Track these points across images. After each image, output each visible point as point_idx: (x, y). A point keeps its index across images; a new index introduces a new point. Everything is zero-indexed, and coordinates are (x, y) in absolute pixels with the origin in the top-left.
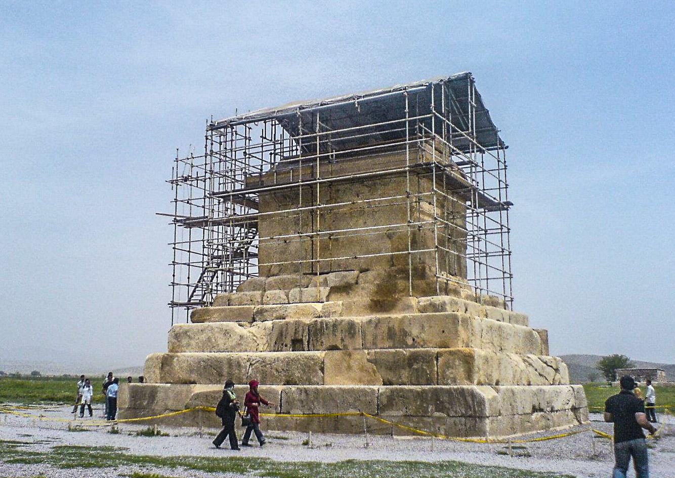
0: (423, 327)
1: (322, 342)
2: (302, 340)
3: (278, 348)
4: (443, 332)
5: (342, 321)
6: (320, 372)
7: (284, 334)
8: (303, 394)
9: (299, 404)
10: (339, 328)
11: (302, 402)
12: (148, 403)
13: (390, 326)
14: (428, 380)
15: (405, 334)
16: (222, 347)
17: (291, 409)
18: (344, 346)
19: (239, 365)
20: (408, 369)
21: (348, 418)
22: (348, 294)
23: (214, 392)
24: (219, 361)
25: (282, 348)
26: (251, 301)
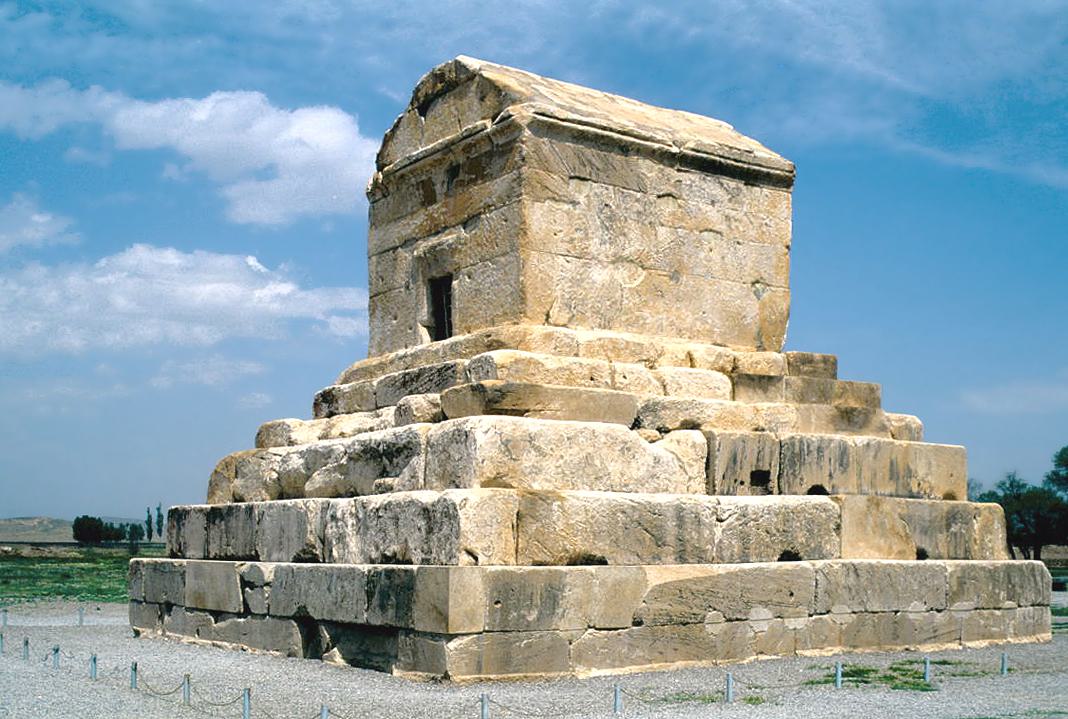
0: (930, 463)
1: (802, 479)
2: (768, 472)
3: (729, 489)
4: (952, 475)
5: (831, 441)
6: (834, 534)
7: (738, 459)
8: (851, 574)
9: (846, 596)
10: (826, 453)
11: (850, 589)
12: (540, 613)
13: (893, 457)
14: (967, 551)
15: (910, 473)
16: (616, 479)
17: (833, 604)
18: (833, 487)
19: (699, 521)
20: (945, 533)
21: (911, 616)
22: (765, 391)
23: (697, 581)
24: (655, 511)
25: (735, 489)
26: (592, 379)
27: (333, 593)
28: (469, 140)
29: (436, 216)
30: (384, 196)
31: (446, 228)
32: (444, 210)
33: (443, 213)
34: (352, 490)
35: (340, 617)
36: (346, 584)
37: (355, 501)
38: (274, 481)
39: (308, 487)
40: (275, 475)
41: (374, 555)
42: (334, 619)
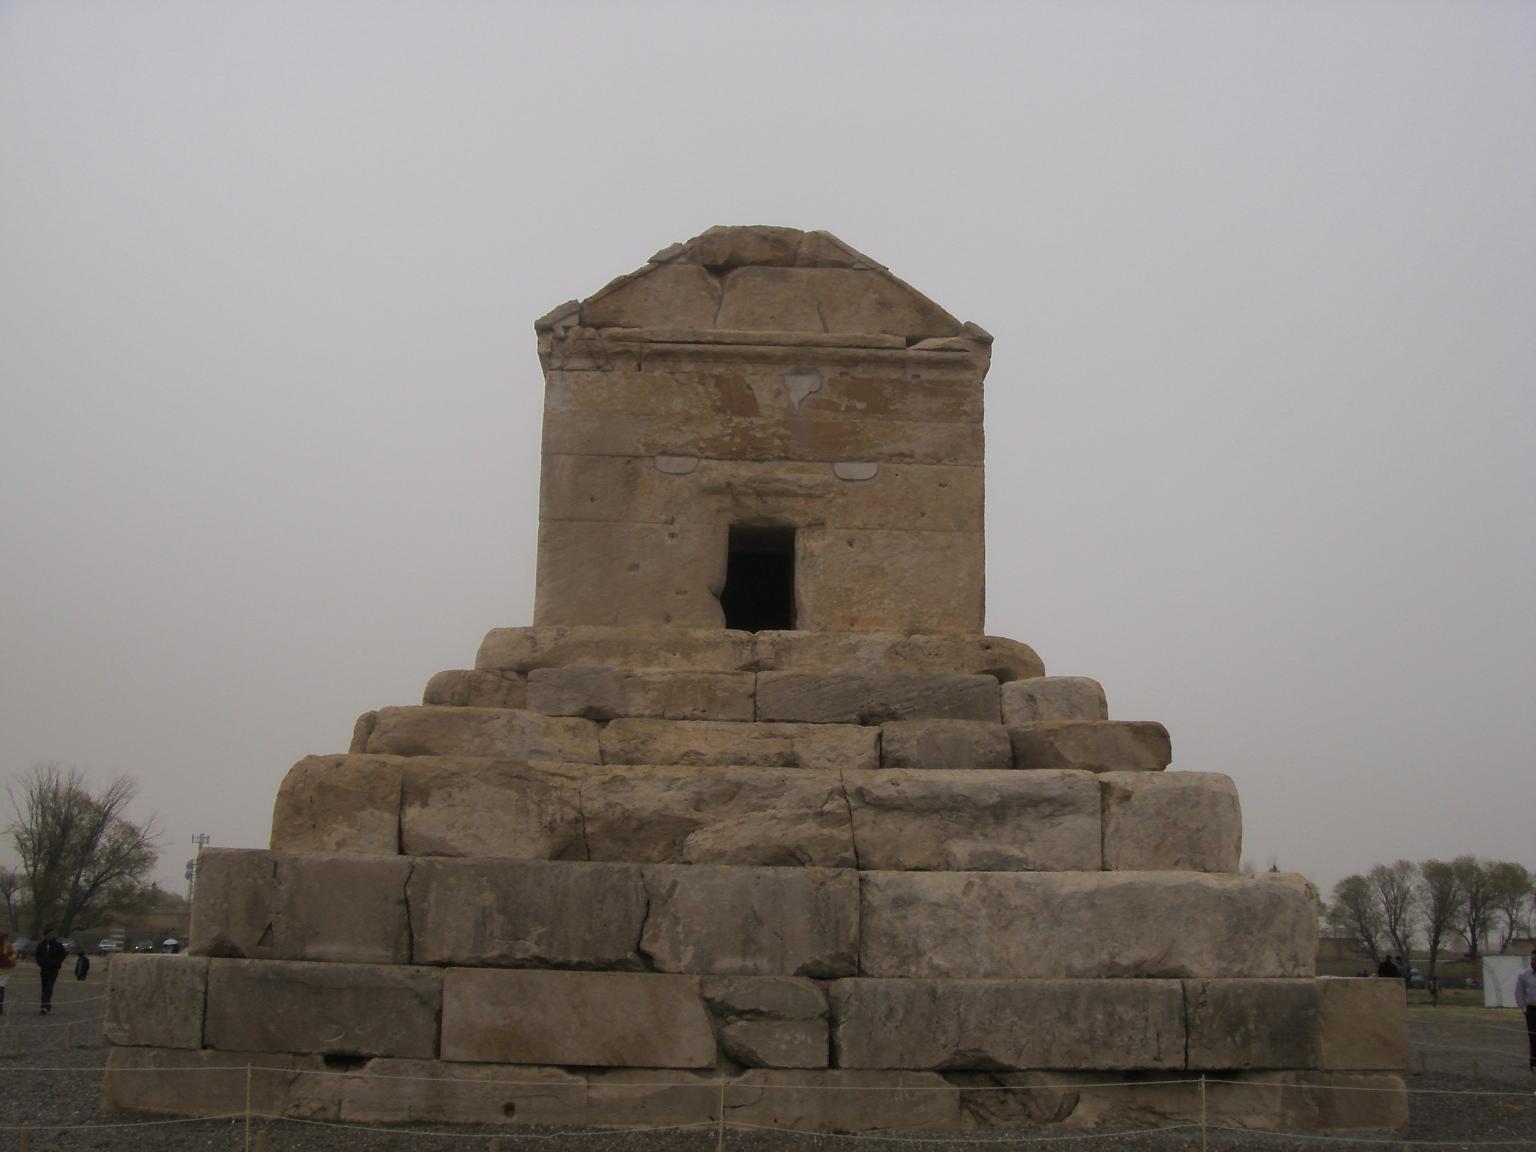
27: (1082, 1024)
28: (863, 352)
29: (759, 435)
30: (599, 368)
31: (787, 458)
32: (782, 431)
33: (781, 438)
34: (849, 854)
35: (1105, 1062)
36: (1119, 1009)
37: (985, 879)
38: (569, 823)
39: (699, 841)
40: (571, 814)
41: (1078, 962)
42: (1084, 1066)
